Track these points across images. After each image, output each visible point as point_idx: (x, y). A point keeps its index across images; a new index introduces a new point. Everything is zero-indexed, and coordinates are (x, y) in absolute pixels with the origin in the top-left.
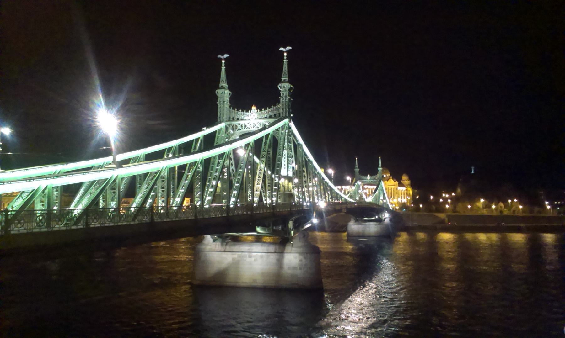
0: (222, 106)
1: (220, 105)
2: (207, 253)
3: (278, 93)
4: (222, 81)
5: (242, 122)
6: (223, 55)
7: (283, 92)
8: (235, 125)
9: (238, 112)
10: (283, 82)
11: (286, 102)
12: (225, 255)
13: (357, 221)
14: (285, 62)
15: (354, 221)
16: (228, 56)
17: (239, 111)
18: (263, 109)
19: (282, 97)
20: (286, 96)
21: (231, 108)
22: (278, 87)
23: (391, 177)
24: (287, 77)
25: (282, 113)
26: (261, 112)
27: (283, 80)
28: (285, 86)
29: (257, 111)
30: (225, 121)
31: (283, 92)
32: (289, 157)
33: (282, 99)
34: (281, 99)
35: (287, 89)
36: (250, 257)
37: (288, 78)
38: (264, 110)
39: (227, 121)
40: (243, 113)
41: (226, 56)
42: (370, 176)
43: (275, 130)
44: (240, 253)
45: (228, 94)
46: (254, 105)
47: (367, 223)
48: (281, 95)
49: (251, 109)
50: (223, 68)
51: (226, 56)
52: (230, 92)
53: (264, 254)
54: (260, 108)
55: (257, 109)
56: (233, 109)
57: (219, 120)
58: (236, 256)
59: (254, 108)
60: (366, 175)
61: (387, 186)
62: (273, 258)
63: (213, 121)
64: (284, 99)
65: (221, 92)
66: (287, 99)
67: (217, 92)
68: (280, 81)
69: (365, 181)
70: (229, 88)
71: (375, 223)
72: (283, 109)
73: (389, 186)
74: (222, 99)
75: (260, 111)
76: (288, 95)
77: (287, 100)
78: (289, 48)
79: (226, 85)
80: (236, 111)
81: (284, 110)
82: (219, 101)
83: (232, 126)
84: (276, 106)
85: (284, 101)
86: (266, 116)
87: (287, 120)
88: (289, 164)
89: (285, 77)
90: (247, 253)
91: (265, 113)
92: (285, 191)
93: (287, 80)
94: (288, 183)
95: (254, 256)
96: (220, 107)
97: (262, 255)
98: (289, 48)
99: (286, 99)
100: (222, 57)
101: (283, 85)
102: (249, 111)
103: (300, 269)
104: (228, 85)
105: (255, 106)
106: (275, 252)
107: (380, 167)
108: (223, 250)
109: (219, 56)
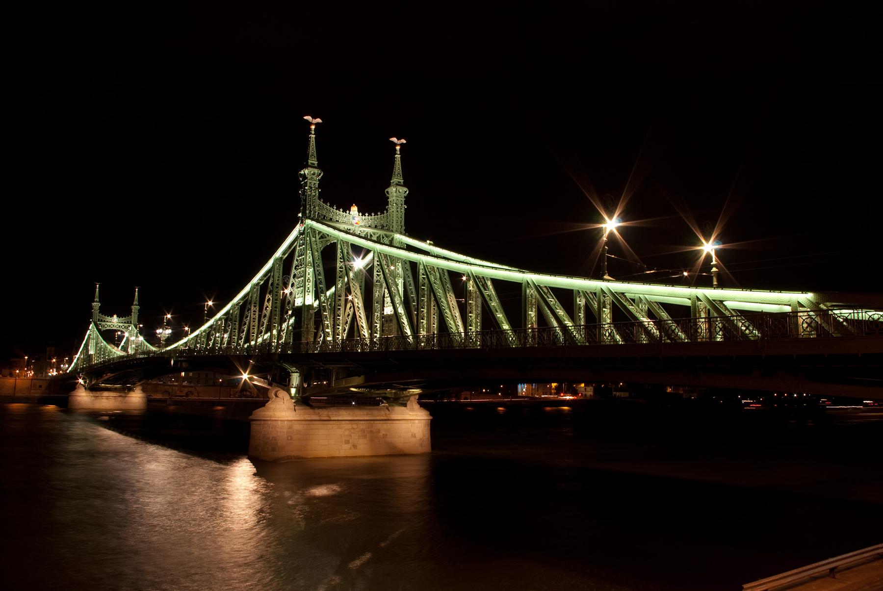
1: (311, 192)
4: (313, 156)
6: (314, 117)
10: (397, 185)
11: (401, 212)
18: (367, 214)
20: (402, 204)
28: (400, 191)
29: (359, 215)
41: (319, 120)
42: (117, 317)
51: (319, 120)
54: (362, 211)
55: (359, 211)
60: (112, 316)
69: (108, 323)
74: (313, 184)
76: (403, 203)
78: (404, 141)
85: (399, 210)
91: (367, 219)
101: (399, 188)
102: (348, 212)
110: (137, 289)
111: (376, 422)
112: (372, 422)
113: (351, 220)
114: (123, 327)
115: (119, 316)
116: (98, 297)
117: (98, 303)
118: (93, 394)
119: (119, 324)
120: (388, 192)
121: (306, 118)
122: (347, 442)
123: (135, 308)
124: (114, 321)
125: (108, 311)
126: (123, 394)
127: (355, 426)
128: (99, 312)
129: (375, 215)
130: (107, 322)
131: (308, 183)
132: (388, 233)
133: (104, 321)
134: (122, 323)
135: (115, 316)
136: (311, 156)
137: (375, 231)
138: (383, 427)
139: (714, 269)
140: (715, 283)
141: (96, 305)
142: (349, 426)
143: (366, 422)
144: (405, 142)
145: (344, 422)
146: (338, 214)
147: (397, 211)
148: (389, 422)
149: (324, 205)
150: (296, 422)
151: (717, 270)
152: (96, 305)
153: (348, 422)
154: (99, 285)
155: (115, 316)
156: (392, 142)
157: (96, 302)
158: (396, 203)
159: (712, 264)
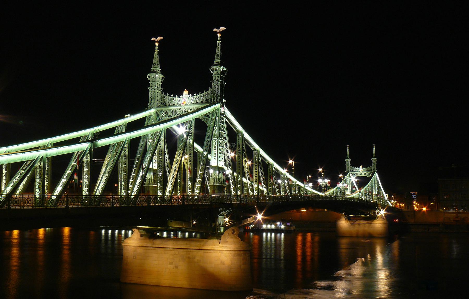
0: (153, 91)
3: (210, 76)
5: (173, 108)
6: (156, 38)
7: (215, 76)
9: (170, 97)
13: (349, 219)
14: (218, 43)
15: (345, 219)
16: (161, 38)
17: (171, 97)
18: (195, 94)
19: (214, 81)
20: (218, 80)
21: (163, 93)
22: (210, 70)
24: (220, 59)
26: (193, 97)
27: (215, 63)
28: (217, 69)
29: (189, 96)
30: (156, 107)
31: (215, 76)
32: (220, 146)
33: (214, 83)
34: (213, 83)
35: (219, 72)
37: (220, 60)
38: (196, 95)
39: (157, 107)
40: (174, 98)
41: (159, 38)
43: (205, 116)
45: (161, 78)
46: (186, 90)
48: (213, 79)
50: (156, 50)
51: (159, 38)
52: (163, 76)
54: (191, 93)
56: (164, 94)
57: (149, 106)
59: (186, 93)
60: (359, 167)
63: (144, 107)
64: (216, 83)
65: (153, 76)
66: (219, 82)
67: (149, 77)
68: (213, 64)
70: (162, 73)
72: (214, 94)
75: (192, 96)
76: (220, 79)
77: (218, 84)
78: (222, 28)
79: (158, 69)
80: (168, 96)
82: (150, 86)
84: (208, 90)
85: (215, 85)
86: (197, 102)
87: (218, 105)
88: (219, 153)
89: (217, 59)
92: (214, 183)
93: (220, 63)
94: (218, 175)
96: (151, 92)
98: (222, 28)
99: (217, 83)
100: (156, 40)
101: (214, 68)
102: (181, 96)
104: (160, 69)
105: (187, 90)
107: (374, 157)
109: (153, 39)
110: (374, 146)
111: (192, 250)
112: (189, 250)
114: (367, 174)
115: (363, 167)
116: (349, 155)
117: (348, 159)
118: (347, 222)
119: (364, 172)
122: (171, 263)
123: (374, 159)
124: (360, 171)
125: (356, 164)
126: (369, 222)
127: (177, 253)
128: (351, 166)
130: (356, 171)
131: (150, 84)
133: (354, 171)
134: (366, 171)
135: (361, 167)
136: (154, 65)
138: (198, 255)
141: (348, 161)
142: (173, 252)
143: (185, 250)
144: (225, 28)
145: (169, 249)
148: (202, 251)
149: (165, 96)
150: (139, 247)
152: (348, 161)
153: (171, 249)
154: (349, 146)
155: (361, 167)
157: (348, 158)
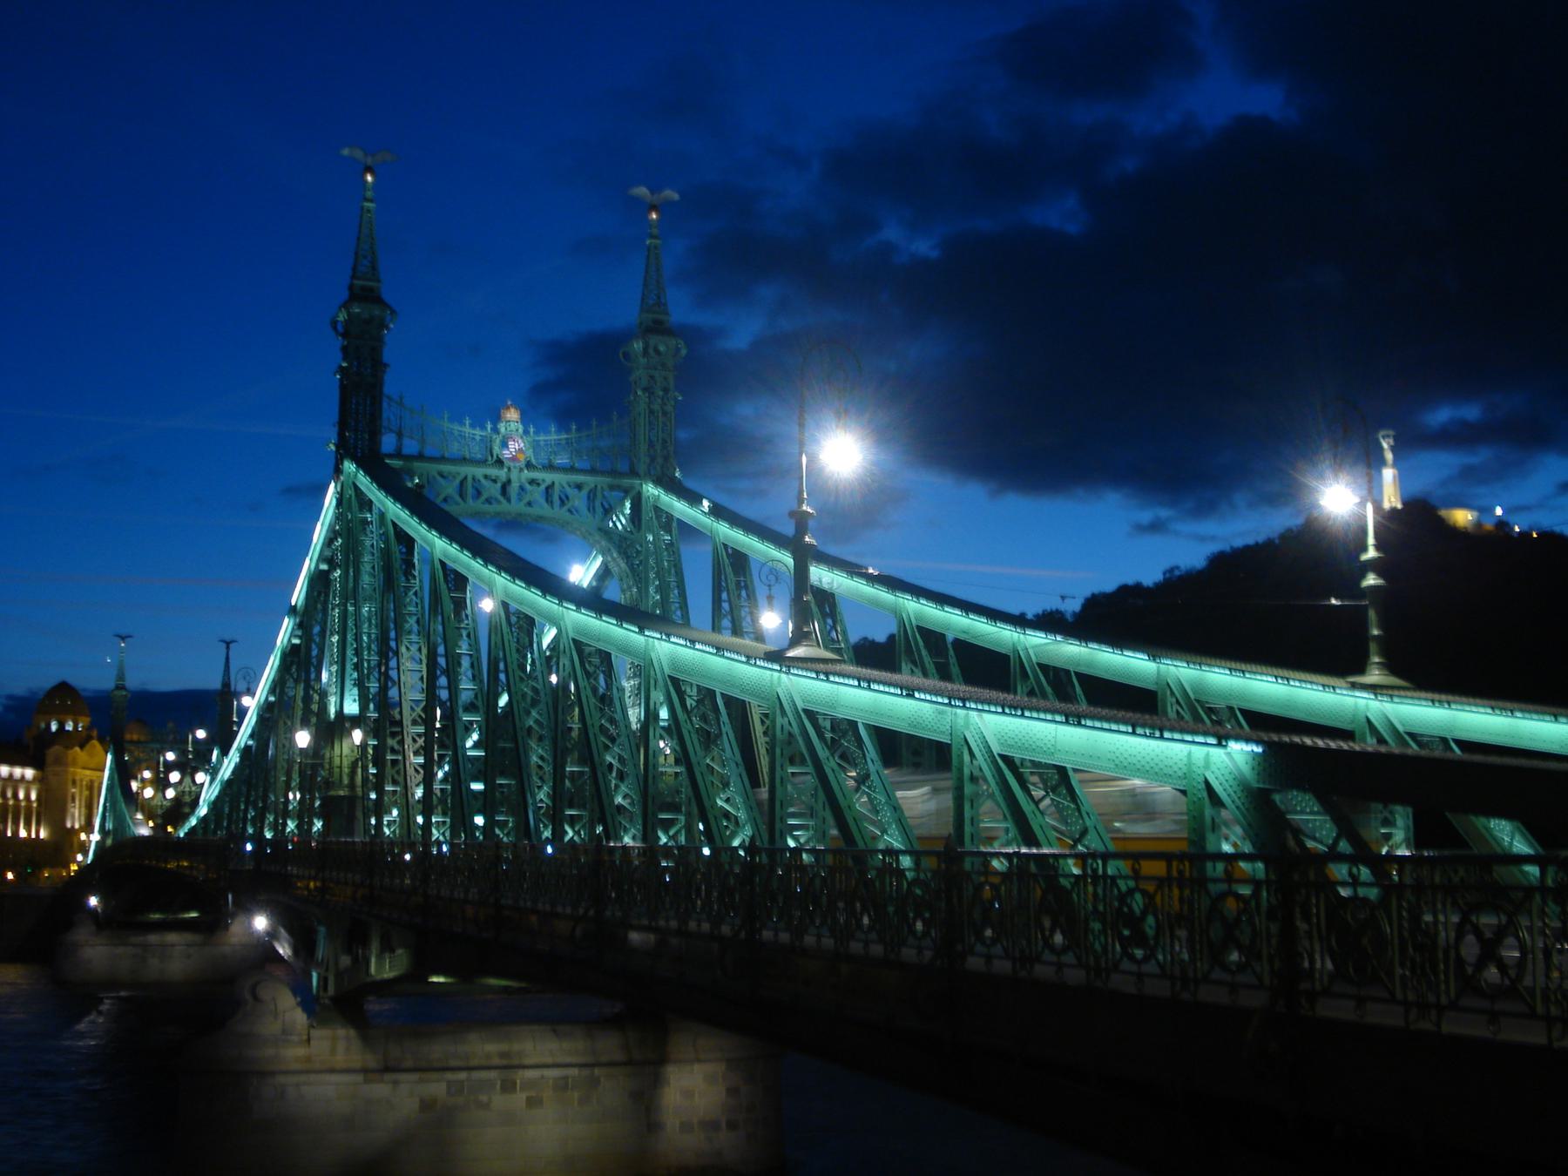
2: (281, 1079)
8: (474, 479)
11: (665, 414)
12: (380, 1089)
20: (666, 390)
23: (95, 733)
25: (653, 459)
28: (662, 348)
29: (526, 432)
33: (649, 398)
36: (508, 1087)
44: (462, 1075)
47: (153, 938)
49: (497, 418)
53: (574, 1072)
55: (525, 419)
58: (436, 1088)
61: (79, 770)
62: (613, 1090)
64: (659, 401)
66: (672, 403)
71: (189, 937)
73: (88, 772)
81: (658, 447)
83: (457, 482)
85: (656, 407)
90: (493, 1074)
95: (528, 1085)
97: (566, 1078)
101: (653, 340)
102: (489, 426)
103: (732, 1125)
105: (516, 406)
106: (625, 1064)
108: (372, 1061)
113: (496, 450)
120: (626, 355)
121: (346, 152)
129: (578, 430)
132: (626, 482)
137: (580, 478)
139: (1371, 580)
140: (1376, 632)
146: (456, 433)
147: (652, 412)
151: (1380, 582)
156: (637, 201)
158: (645, 390)
159: (1364, 557)
